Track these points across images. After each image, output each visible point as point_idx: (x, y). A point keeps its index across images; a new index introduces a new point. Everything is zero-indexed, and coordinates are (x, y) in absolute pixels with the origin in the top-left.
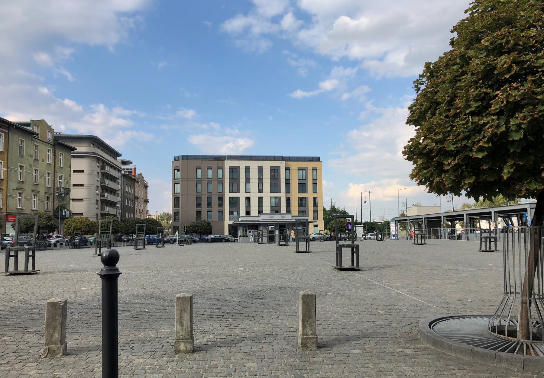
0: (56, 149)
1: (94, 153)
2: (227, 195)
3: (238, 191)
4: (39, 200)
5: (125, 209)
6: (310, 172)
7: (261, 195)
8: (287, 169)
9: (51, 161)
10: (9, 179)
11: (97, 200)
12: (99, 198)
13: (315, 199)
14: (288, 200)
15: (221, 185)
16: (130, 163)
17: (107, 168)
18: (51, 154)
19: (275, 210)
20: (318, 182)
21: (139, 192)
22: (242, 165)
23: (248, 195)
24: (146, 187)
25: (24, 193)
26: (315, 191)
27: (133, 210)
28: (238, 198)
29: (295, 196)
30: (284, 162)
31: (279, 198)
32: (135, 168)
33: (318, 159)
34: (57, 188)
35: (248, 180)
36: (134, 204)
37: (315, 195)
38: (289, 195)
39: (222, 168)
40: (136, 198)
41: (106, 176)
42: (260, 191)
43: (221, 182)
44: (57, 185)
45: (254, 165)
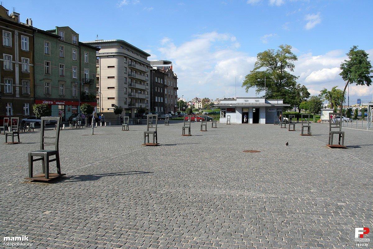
0: (81, 50)
1: (121, 53)
5: (153, 94)
10: (36, 72)
16: (170, 63)
17: (134, 63)
21: (167, 81)
24: (175, 78)
27: (162, 95)
32: (172, 66)
36: (164, 91)
40: (166, 86)
41: (133, 69)
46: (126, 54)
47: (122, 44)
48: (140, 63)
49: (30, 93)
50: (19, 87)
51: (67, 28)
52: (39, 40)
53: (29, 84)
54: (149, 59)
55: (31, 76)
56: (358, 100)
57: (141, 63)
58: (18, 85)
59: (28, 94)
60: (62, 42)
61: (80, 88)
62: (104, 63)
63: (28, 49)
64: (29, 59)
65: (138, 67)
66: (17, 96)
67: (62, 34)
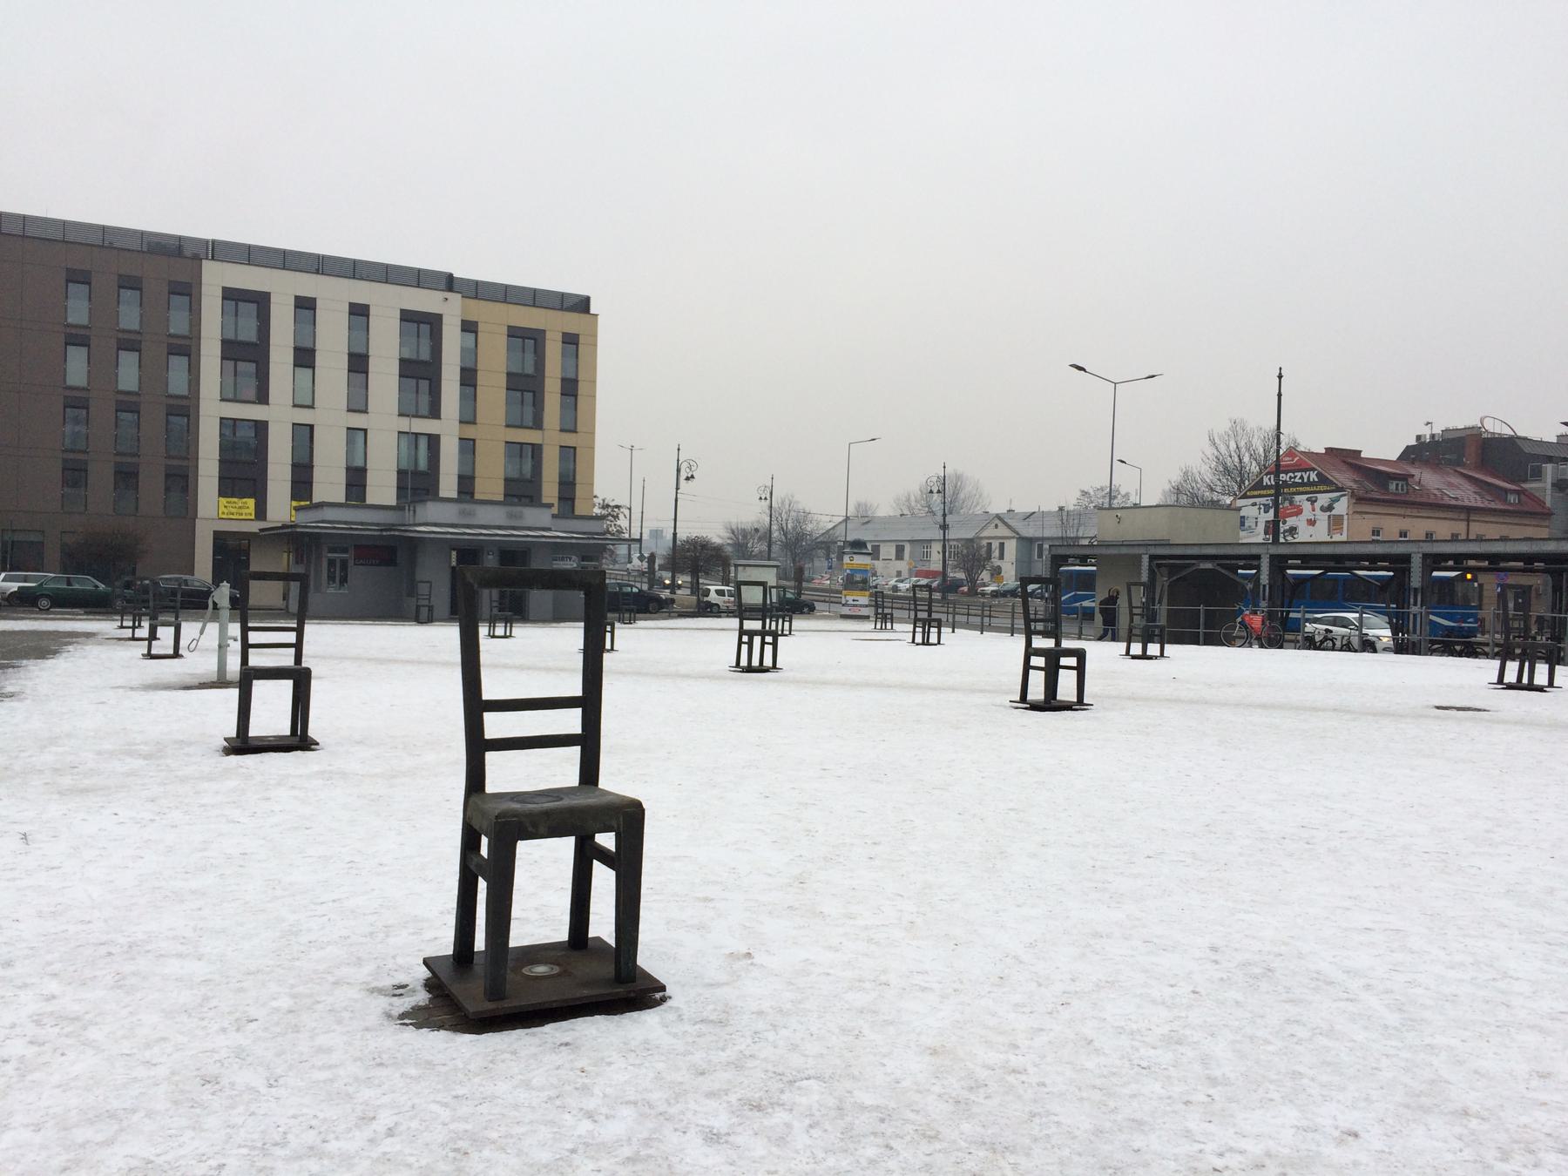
2: (212, 411)
3: (263, 397)
6: (553, 350)
7: (358, 421)
8: (469, 327)
13: (569, 454)
14: (468, 447)
19: (417, 483)
20: (582, 389)
23: (304, 417)
26: (570, 427)
28: (261, 428)
29: (494, 432)
30: (455, 298)
31: (434, 441)
33: (582, 305)
35: (305, 357)
37: (569, 440)
38: (470, 432)
39: (188, 290)
42: (358, 404)
43: (187, 348)
45: (334, 296)
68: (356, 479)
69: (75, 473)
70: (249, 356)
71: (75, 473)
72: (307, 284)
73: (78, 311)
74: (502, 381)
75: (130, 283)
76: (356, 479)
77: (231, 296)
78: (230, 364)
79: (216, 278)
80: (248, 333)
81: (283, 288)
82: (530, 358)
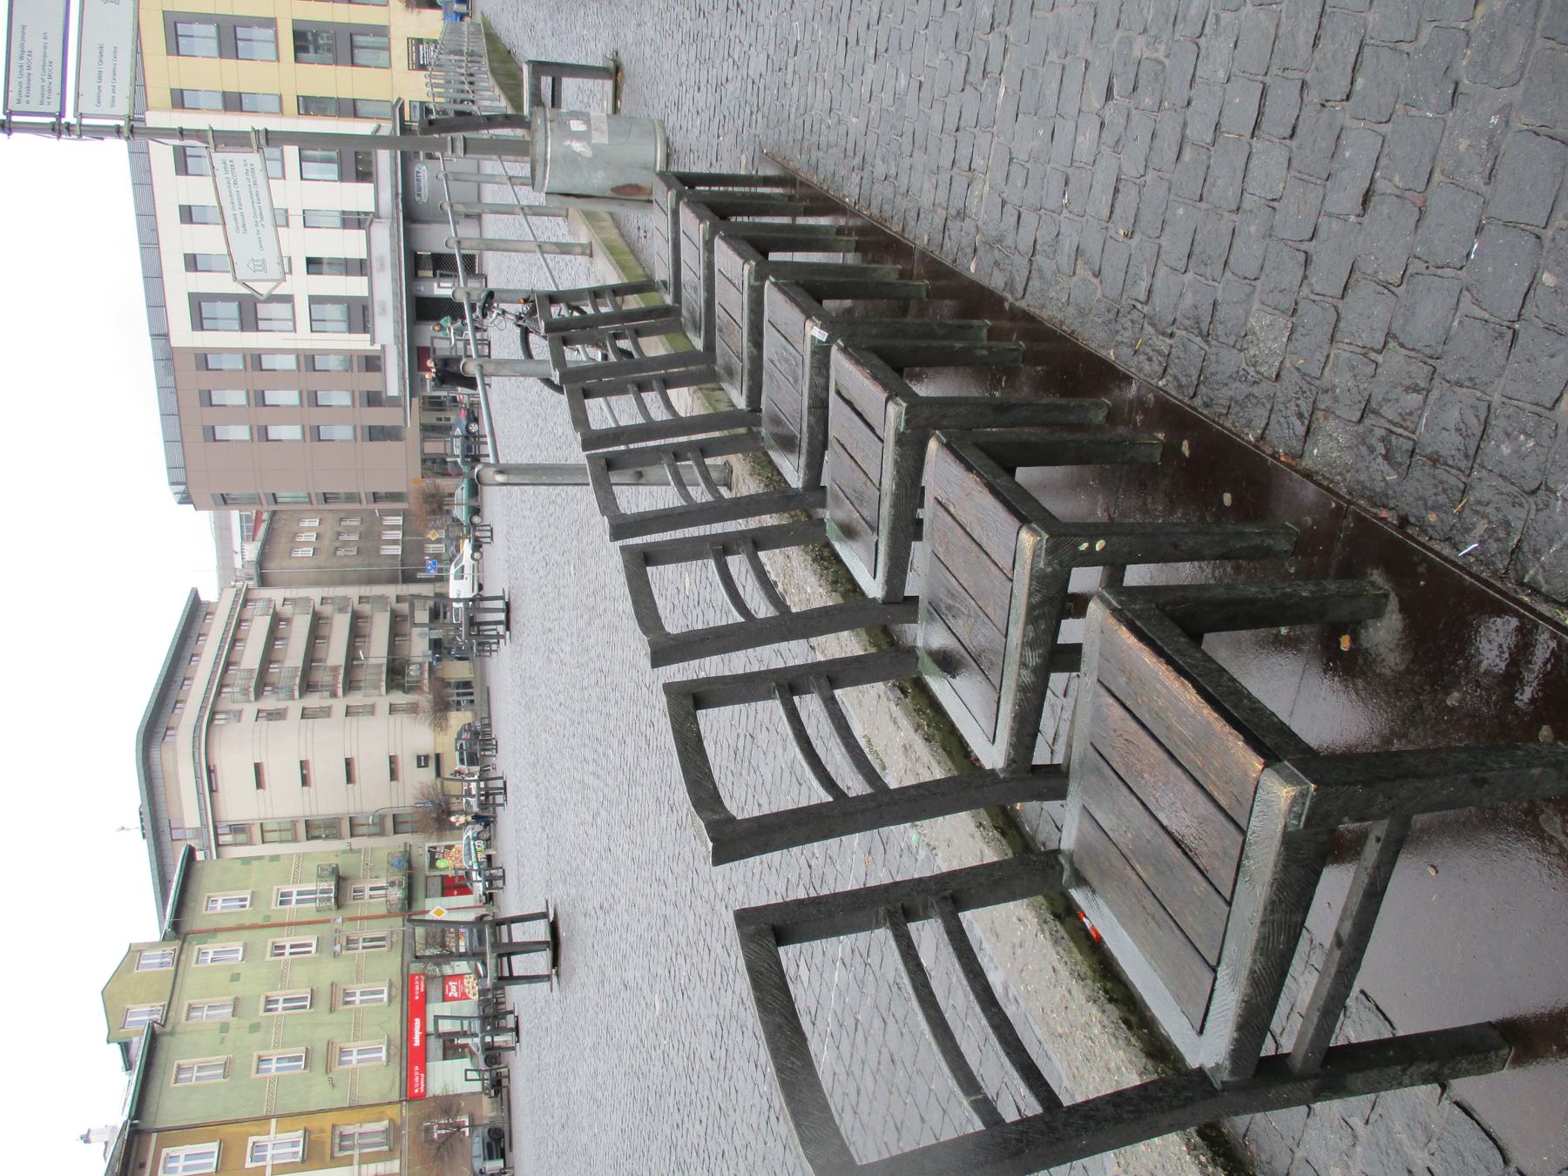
1: (197, 728)
2: (305, 339)
4: (358, 981)
9: (236, 944)
11: (349, 712)
12: (339, 705)
15: (268, 362)
18: (211, 948)
22: (179, 285)
25: (339, 1043)
28: (314, 300)
34: (318, 910)
39: (202, 359)
43: (255, 360)
44: (309, 910)
45: (176, 239)
46: (200, 717)
47: (154, 730)
48: (234, 641)
49: (380, 1120)
50: (360, 1164)
51: (107, 995)
52: (170, 1108)
53: (349, 1130)
54: (208, 595)
55: (315, 1123)
56: (419, 766)
57: (235, 639)
58: (356, 1167)
59: (386, 1131)
60: (171, 1013)
61: (355, 919)
62: (239, 802)
63: (213, 1147)
64: (252, 1139)
65: (251, 656)
66: (397, 1170)
67: (142, 1015)
68: (353, 221)
69: (377, 434)
70: (248, 313)
71: (377, 434)
72: (172, 264)
73: (240, 433)
74: (230, 63)
75: (206, 399)
76: (353, 221)
77: (198, 323)
78: (262, 325)
79: (183, 335)
80: (232, 309)
81: (179, 285)
82: (197, 29)
